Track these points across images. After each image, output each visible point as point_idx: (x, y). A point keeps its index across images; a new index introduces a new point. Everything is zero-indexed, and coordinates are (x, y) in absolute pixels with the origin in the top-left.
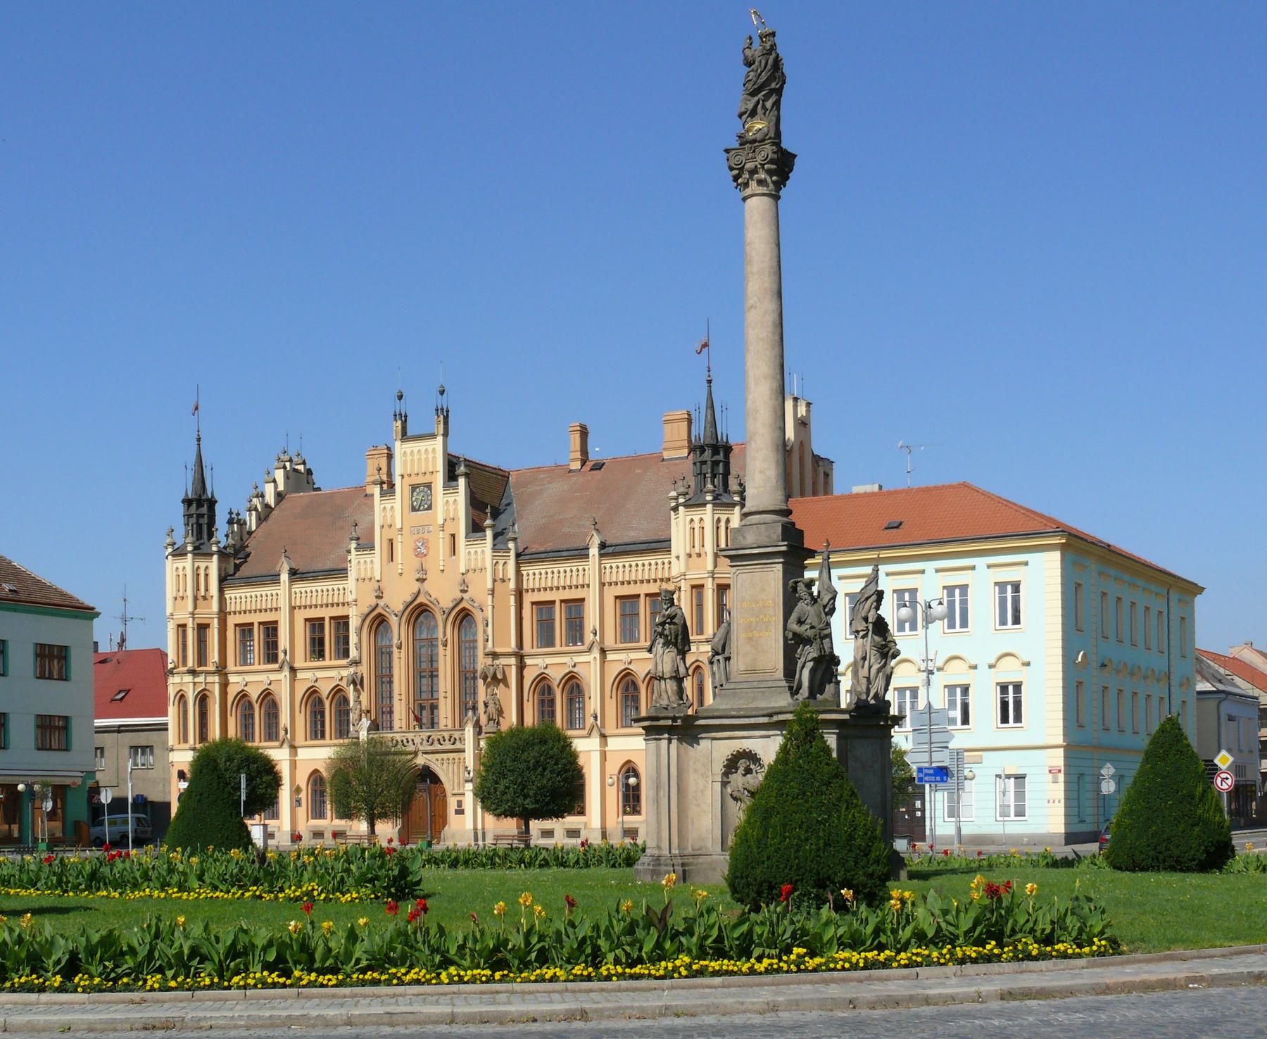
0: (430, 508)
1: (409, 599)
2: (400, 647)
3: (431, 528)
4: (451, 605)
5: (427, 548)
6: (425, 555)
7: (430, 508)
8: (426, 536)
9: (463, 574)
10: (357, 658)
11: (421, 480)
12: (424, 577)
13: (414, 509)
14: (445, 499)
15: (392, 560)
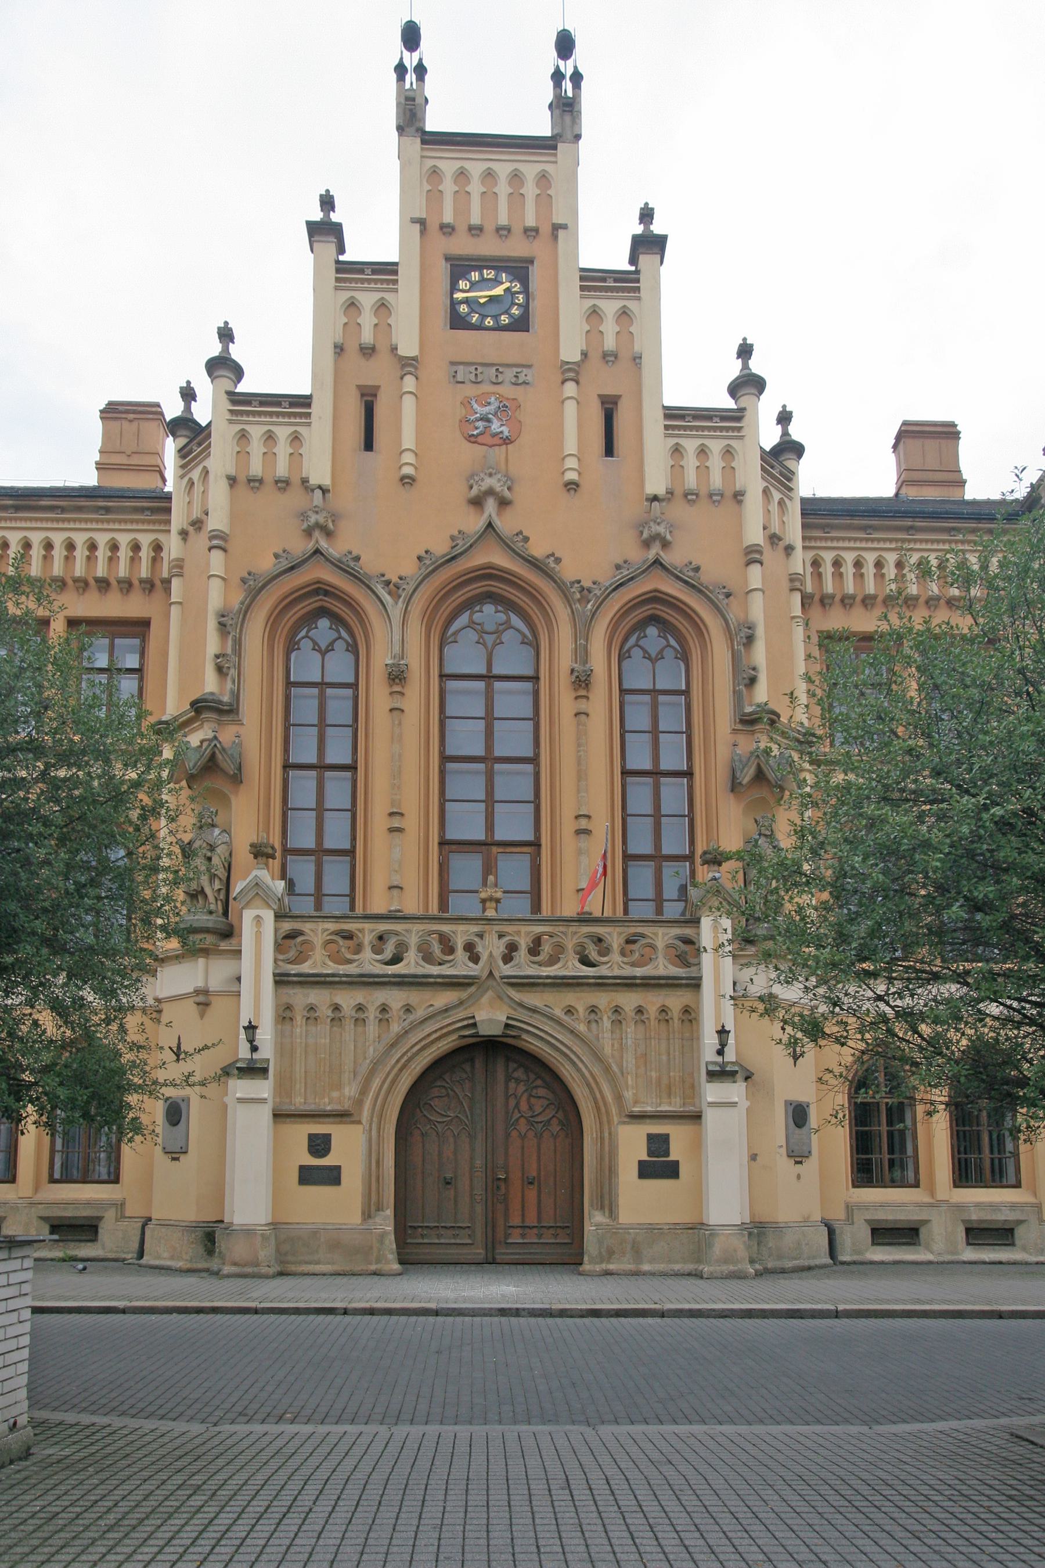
0: (521, 324)
1: (441, 548)
2: (397, 677)
3: (526, 375)
4: (606, 576)
5: (518, 426)
6: (507, 441)
7: (521, 324)
8: (507, 390)
9: (655, 498)
10: (226, 699)
11: (488, 247)
12: (507, 494)
13: (458, 322)
14: (590, 303)
15: (369, 445)
